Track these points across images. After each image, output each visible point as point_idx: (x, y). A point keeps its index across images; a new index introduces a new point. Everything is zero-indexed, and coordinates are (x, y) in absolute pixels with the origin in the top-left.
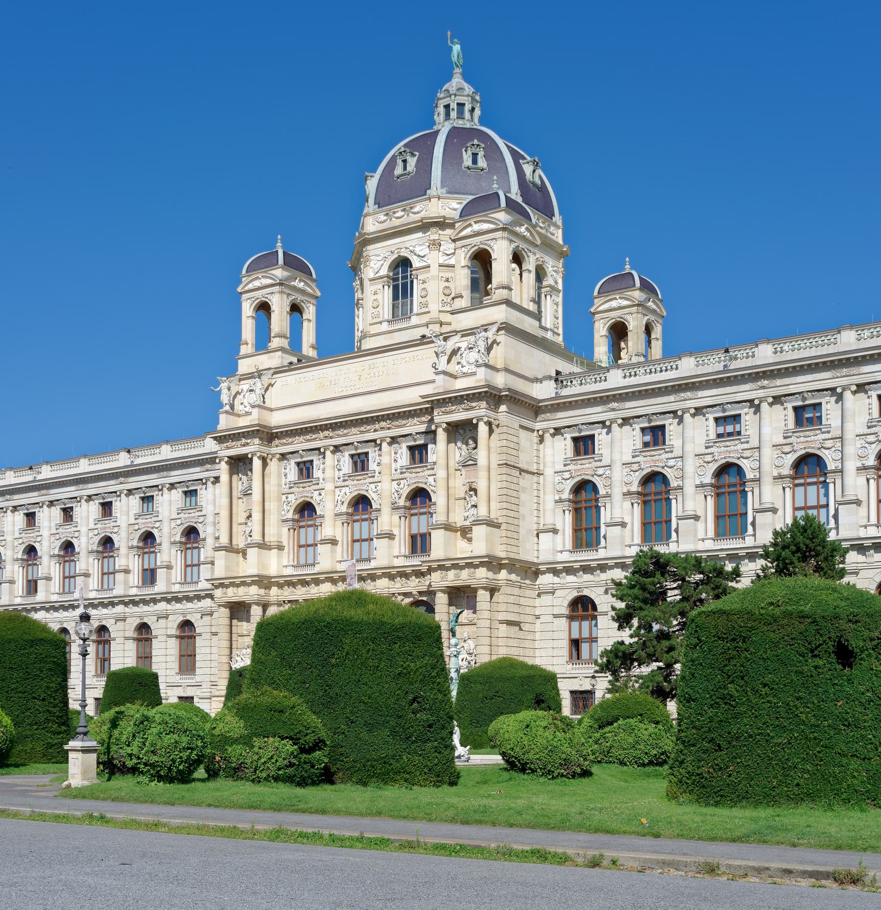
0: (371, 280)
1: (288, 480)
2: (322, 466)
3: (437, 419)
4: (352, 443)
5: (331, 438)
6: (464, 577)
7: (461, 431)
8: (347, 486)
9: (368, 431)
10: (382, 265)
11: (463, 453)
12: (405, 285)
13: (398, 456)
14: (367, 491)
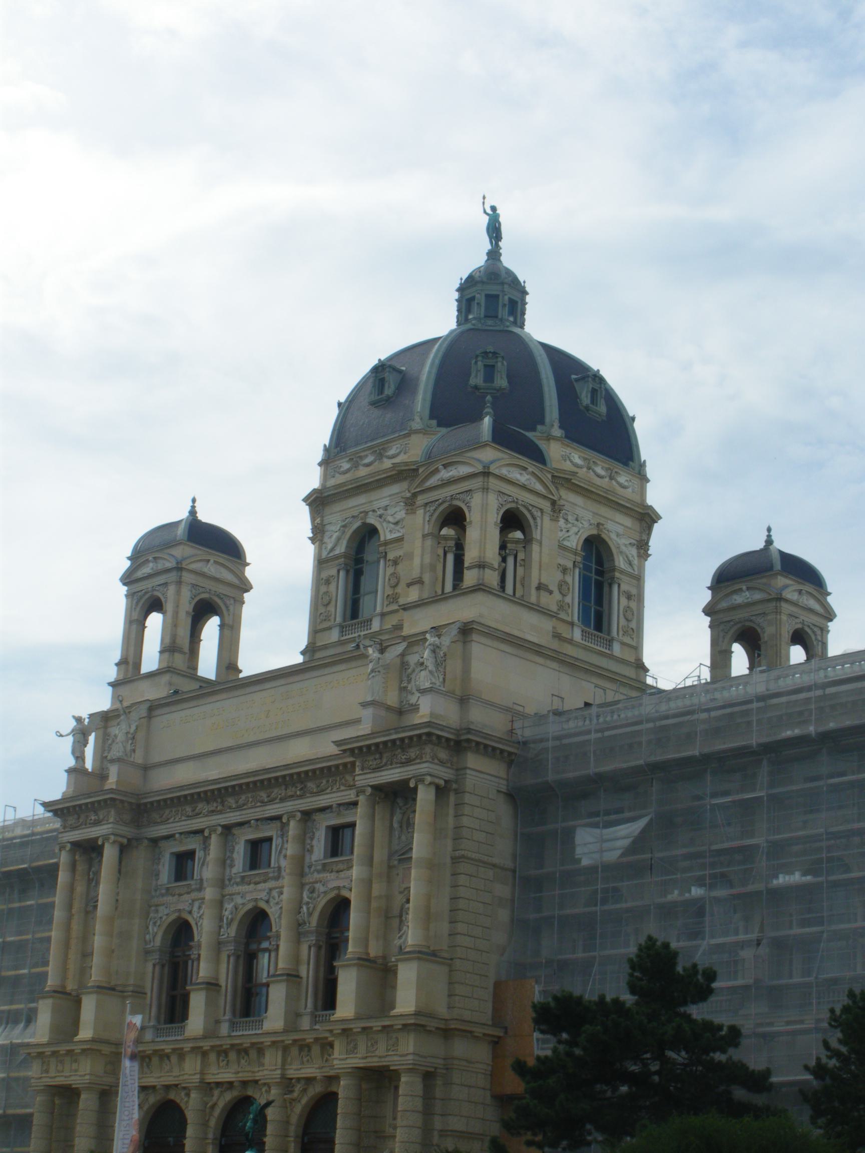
1: (159, 883)
4: (248, 822)
5: (220, 812)
7: (400, 801)
8: (239, 893)
9: (272, 801)
10: (339, 539)
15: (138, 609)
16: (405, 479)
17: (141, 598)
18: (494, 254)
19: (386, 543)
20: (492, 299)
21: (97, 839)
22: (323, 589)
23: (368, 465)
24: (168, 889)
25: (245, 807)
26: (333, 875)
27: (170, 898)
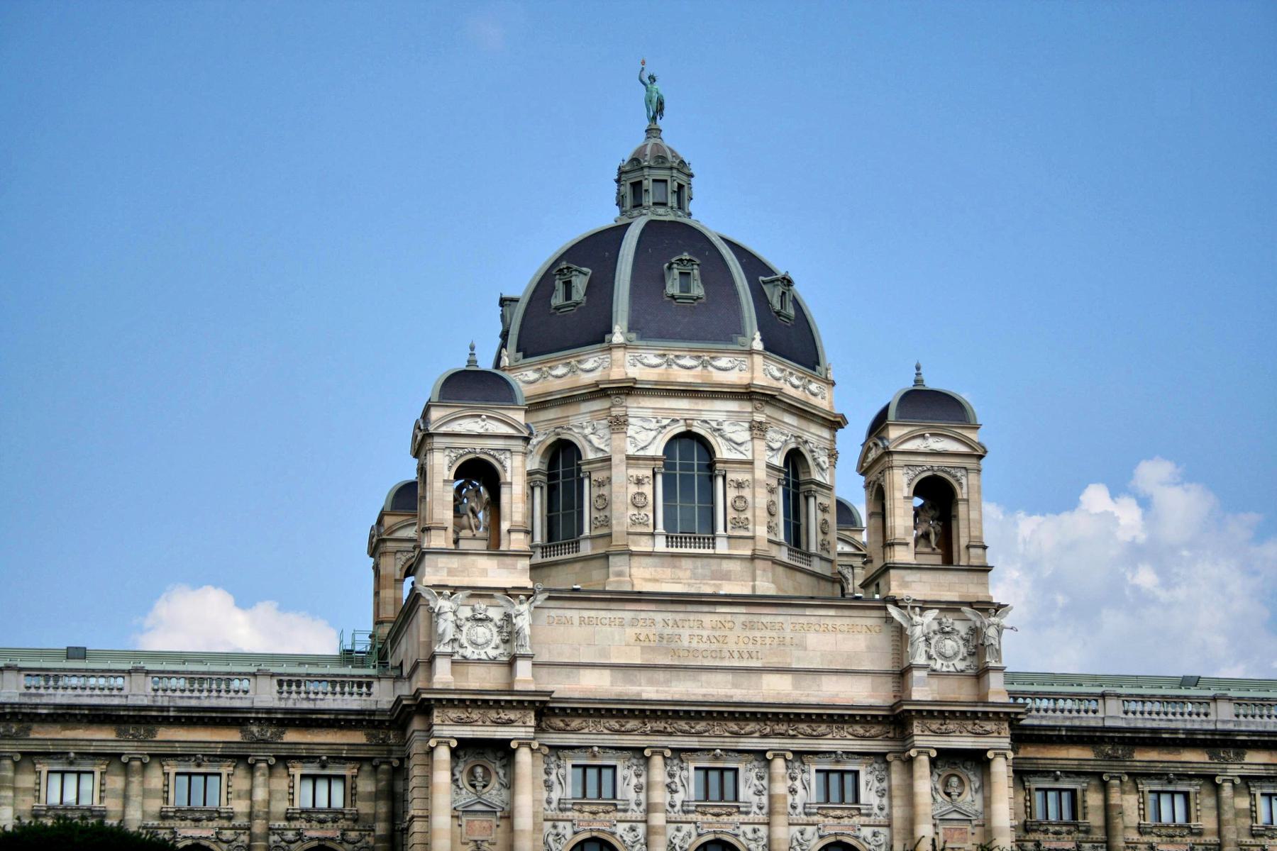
0: (628, 458)
2: (634, 781)
3: (920, 741)
5: (670, 734)
8: (695, 823)
10: (655, 438)
11: (939, 799)
12: (687, 480)
13: (798, 784)
14: (736, 835)
16: (751, 400)
17: (461, 456)
19: (726, 462)
22: (633, 489)
25: (707, 734)
26: (830, 821)
27: (577, 814)
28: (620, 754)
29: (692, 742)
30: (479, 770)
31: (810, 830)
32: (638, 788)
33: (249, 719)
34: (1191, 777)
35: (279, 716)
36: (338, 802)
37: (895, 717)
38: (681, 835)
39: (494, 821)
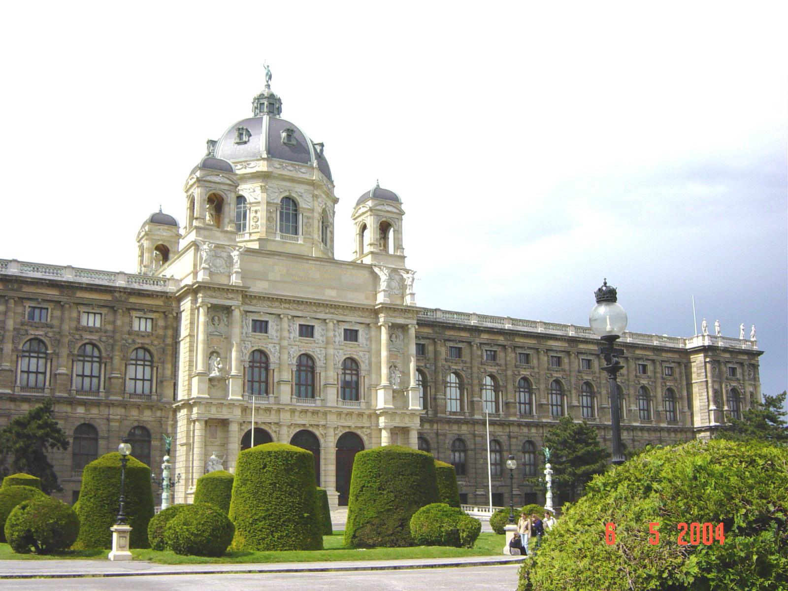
2: (275, 328)
5: (291, 310)
6: (407, 422)
9: (321, 312)
15: (207, 196)
18: (268, 86)
19: (303, 208)
20: (271, 104)
21: (231, 306)
23: (291, 171)
24: (252, 335)
26: (349, 349)
27: (253, 339)
28: (271, 315)
29: (299, 314)
30: (216, 318)
31: (341, 351)
32: (277, 331)
33: (115, 291)
34: (463, 342)
35: (129, 291)
36: (149, 329)
37: (375, 310)
38: (293, 350)
39: (222, 339)
